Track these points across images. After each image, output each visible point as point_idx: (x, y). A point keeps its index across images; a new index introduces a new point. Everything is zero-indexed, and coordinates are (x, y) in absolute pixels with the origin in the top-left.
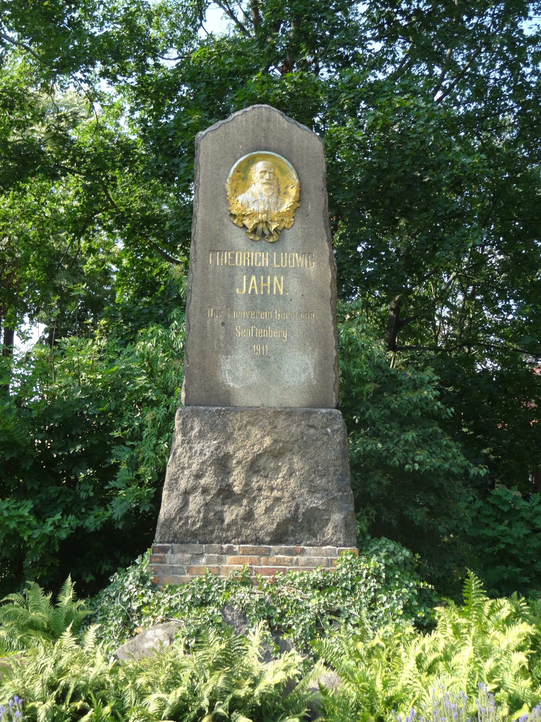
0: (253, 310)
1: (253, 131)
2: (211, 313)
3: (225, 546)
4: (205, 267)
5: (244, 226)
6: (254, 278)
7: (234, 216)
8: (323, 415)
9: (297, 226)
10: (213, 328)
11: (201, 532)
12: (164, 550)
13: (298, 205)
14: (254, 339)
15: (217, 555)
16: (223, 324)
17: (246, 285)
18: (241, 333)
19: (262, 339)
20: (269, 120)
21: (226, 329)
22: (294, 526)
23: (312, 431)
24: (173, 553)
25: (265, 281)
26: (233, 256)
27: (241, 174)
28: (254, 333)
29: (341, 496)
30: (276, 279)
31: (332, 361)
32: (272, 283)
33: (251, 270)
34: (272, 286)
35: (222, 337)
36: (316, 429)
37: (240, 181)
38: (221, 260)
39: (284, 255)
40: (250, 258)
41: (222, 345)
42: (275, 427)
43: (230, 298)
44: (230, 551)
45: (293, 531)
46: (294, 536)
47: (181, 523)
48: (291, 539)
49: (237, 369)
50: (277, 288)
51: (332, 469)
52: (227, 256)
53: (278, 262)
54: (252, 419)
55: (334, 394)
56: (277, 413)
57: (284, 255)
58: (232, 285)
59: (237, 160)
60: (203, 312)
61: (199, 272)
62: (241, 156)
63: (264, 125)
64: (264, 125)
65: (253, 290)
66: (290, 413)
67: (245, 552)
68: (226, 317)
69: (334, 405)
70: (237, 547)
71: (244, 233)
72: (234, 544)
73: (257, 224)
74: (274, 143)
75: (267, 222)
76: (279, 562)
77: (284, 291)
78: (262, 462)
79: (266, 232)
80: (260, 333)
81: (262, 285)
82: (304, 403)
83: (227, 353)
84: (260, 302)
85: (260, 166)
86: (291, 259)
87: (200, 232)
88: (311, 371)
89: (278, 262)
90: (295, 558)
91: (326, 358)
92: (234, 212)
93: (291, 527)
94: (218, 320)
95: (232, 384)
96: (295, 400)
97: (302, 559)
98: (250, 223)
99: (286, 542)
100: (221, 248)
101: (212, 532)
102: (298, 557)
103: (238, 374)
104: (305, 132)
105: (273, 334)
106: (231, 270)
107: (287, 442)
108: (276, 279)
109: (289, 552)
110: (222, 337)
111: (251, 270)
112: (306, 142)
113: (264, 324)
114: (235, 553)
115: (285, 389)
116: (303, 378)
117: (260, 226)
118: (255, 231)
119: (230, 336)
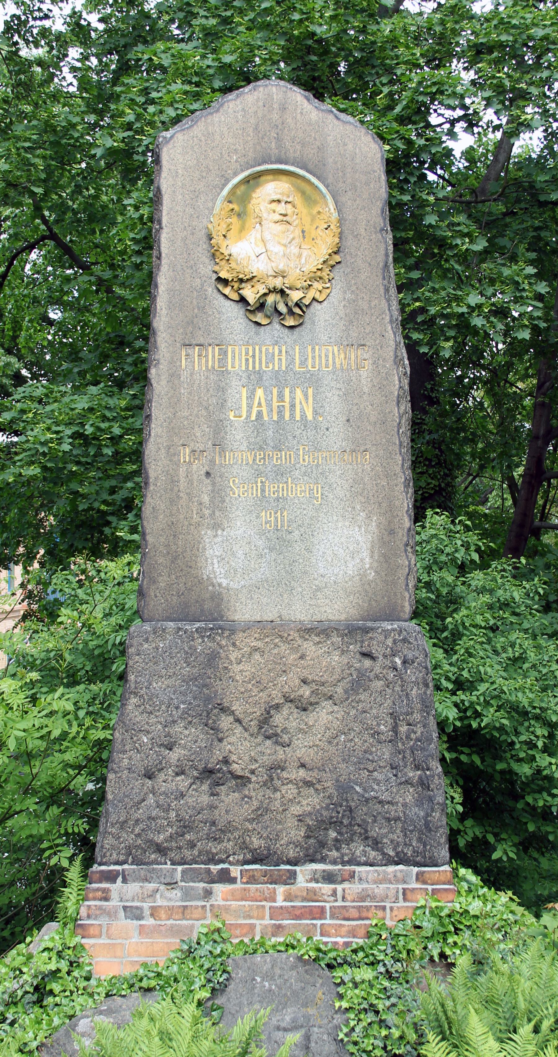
0: (261, 448)
1: (256, 128)
2: (185, 454)
3: (215, 868)
4: (174, 376)
5: (243, 300)
6: (260, 392)
7: (225, 282)
8: (387, 634)
9: (336, 294)
10: (191, 482)
11: (174, 844)
12: (111, 877)
13: (337, 258)
15: (202, 885)
16: (208, 474)
18: (241, 491)
19: (278, 499)
20: (283, 108)
21: (214, 484)
22: (339, 833)
23: (367, 663)
24: (125, 881)
25: (281, 397)
26: (224, 353)
27: (235, 206)
28: (263, 491)
29: (420, 777)
30: (299, 393)
31: (402, 536)
32: (293, 399)
33: (256, 378)
34: (293, 406)
35: (206, 499)
36: (373, 658)
37: (234, 220)
39: (313, 349)
40: (254, 356)
41: (207, 512)
42: (302, 657)
44: (225, 877)
45: (336, 840)
46: (338, 849)
47: (137, 831)
48: (334, 854)
49: (233, 554)
50: (303, 411)
51: (403, 729)
52: (213, 353)
53: (303, 363)
54: (259, 644)
55: (407, 595)
56: (307, 631)
57: (313, 349)
58: (222, 405)
59: (227, 181)
60: (172, 454)
61: (164, 383)
62: (235, 174)
63: (275, 116)
64: (275, 116)
65: (259, 414)
66: (319, 630)
67: (252, 880)
68: (212, 461)
69: (407, 616)
70: (235, 871)
71: (242, 311)
72: (231, 863)
73: (265, 295)
74: (293, 150)
75: (282, 292)
76: (312, 895)
77: (315, 413)
78: (278, 719)
79: (282, 308)
81: (275, 404)
82: (353, 612)
83: (216, 526)
85: (272, 188)
86: (327, 356)
87: (164, 312)
88: (366, 554)
89: (303, 363)
90: (339, 888)
91: (392, 532)
92: (223, 275)
93: (333, 834)
94: (199, 468)
95: (224, 582)
96: (337, 608)
97: (353, 888)
99: (323, 860)
100: (201, 341)
101: (192, 845)
102: (346, 885)
104: (348, 127)
107: (323, 684)
108: (299, 393)
109: (329, 878)
110: (206, 499)
112: (350, 146)
113: (280, 473)
114: (233, 881)
115: (319, 589)
116: (351, 568)
117: (271, 299)
118: (261, 306)
119: (219, 498)
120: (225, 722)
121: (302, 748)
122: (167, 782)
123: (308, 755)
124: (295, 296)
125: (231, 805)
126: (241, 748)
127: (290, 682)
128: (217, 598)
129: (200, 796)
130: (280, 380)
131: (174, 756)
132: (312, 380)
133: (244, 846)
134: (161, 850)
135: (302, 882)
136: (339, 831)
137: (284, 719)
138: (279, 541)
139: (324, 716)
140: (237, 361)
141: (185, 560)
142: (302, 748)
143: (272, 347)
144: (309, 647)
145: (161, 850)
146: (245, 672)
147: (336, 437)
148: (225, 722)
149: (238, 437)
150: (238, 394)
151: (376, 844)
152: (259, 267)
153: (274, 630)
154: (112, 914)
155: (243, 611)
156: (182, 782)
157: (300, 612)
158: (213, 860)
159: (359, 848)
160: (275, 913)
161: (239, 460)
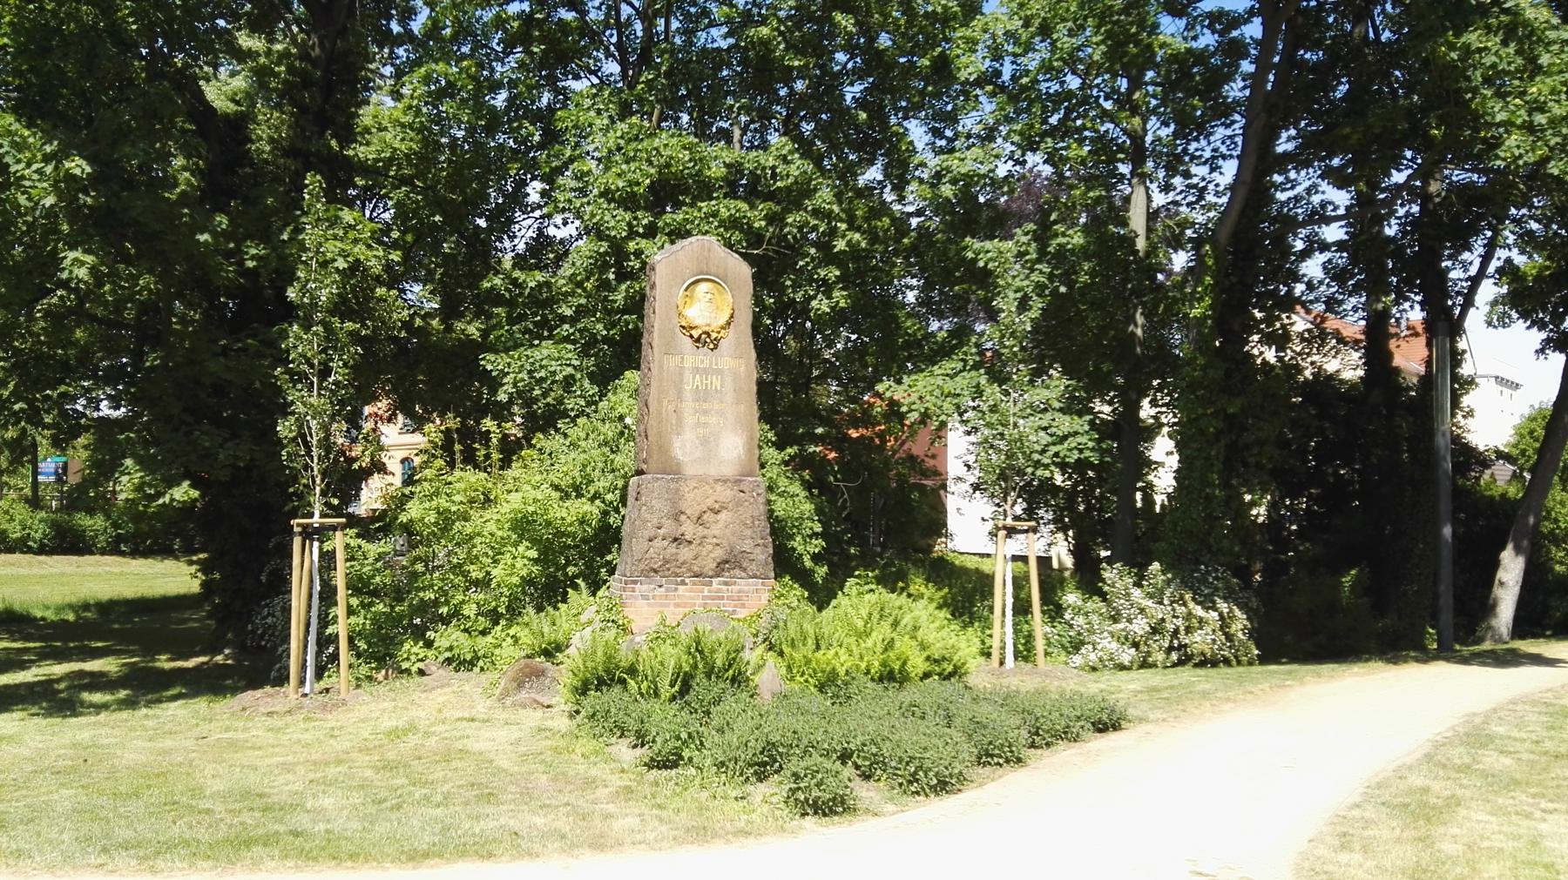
4: (661, 367)
12: (635, 582)
14: (698, 424)
17: (691, 383)
18: (689, 420)
33: (696, 370)
38: (671, 362)
43: (680, 393)
44: (683, 583)
60: (660, 402)
74: (713, 269)
76: (719, 591)
80: (703, 419)
84: (702, 395)
85: (703, 286)
94: (671, 408)
96: (729, 470)
97: (735, 588)
98: (695, 333)
103: (684, 448)
105: (713, 420)
106: (681, 372)
109: (726, 584)
111: (696, 370)
113: (705, 412)
116: (735, 454)
120: (683, 518)
121: (715, 530)
122: (658, 543)
123: (716, 532)
124: (714, 335)
125: (685, 553)
126: (688, 529)
127: (710, 502)
128: (678, 464)
129: (672, 549)
130: (706, 372)
131: (661, 532)
132: (720, 372)
133: (689, 570)
134: (656, 571)
135: (715, 586)
136: (728, 564)
137: (708, 517)
138: (705, 441)
139: (723, 516)
140: (689, 361)
141: (664, 449)
142: (715, 530)
143: (703, 357)
144: (719, 487)
145: (656, 571)
146: (693, 501)
147: (729, 397)
148: (683, 518)
149: (688, 395)
150: (688, 376)
151: (745, 570)
152: (697, 322)
153: (702, 480)
154: (636, 598)
155: (689, 471)
156: (666, 543)
157: (713, 471)
158: (677, 575)
159: (737, 572)
160: (704, 598)
161: (688, 405)
